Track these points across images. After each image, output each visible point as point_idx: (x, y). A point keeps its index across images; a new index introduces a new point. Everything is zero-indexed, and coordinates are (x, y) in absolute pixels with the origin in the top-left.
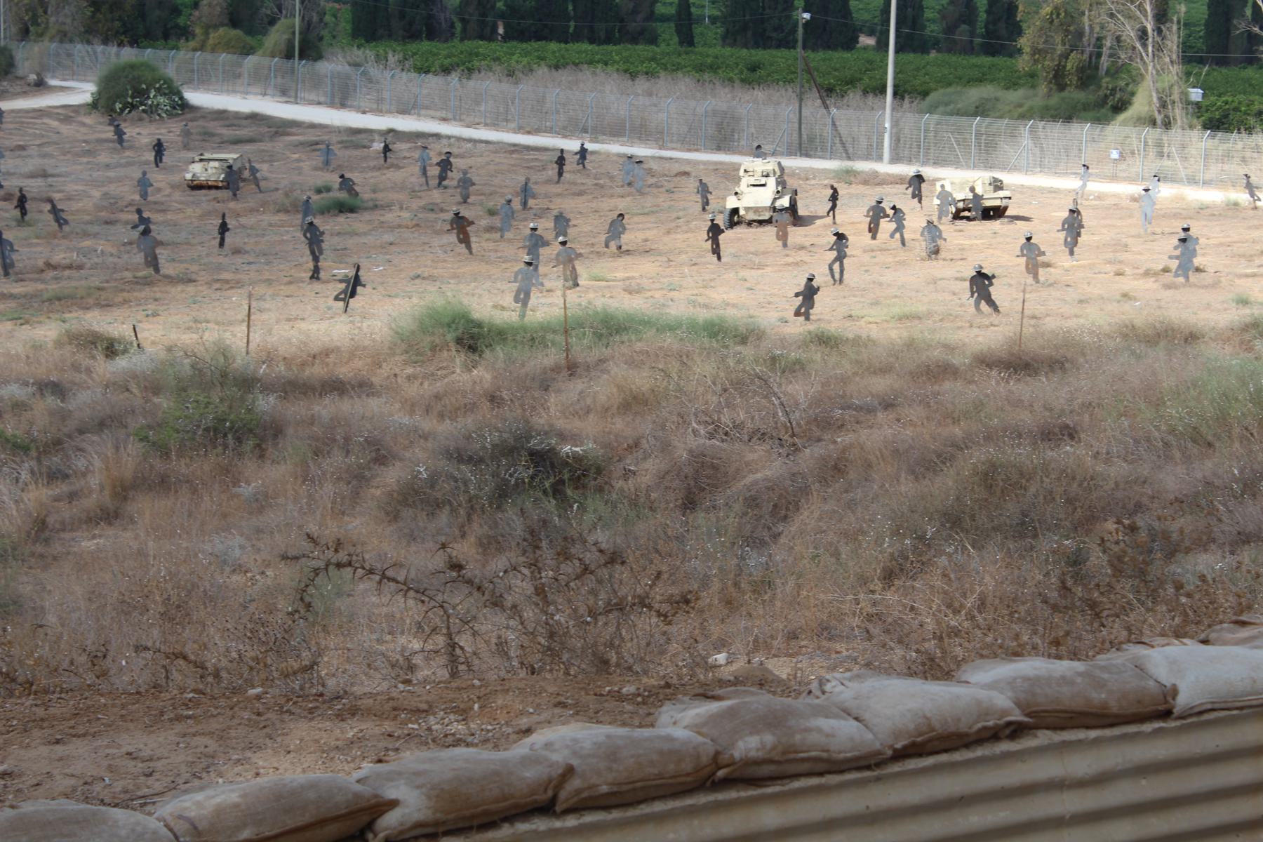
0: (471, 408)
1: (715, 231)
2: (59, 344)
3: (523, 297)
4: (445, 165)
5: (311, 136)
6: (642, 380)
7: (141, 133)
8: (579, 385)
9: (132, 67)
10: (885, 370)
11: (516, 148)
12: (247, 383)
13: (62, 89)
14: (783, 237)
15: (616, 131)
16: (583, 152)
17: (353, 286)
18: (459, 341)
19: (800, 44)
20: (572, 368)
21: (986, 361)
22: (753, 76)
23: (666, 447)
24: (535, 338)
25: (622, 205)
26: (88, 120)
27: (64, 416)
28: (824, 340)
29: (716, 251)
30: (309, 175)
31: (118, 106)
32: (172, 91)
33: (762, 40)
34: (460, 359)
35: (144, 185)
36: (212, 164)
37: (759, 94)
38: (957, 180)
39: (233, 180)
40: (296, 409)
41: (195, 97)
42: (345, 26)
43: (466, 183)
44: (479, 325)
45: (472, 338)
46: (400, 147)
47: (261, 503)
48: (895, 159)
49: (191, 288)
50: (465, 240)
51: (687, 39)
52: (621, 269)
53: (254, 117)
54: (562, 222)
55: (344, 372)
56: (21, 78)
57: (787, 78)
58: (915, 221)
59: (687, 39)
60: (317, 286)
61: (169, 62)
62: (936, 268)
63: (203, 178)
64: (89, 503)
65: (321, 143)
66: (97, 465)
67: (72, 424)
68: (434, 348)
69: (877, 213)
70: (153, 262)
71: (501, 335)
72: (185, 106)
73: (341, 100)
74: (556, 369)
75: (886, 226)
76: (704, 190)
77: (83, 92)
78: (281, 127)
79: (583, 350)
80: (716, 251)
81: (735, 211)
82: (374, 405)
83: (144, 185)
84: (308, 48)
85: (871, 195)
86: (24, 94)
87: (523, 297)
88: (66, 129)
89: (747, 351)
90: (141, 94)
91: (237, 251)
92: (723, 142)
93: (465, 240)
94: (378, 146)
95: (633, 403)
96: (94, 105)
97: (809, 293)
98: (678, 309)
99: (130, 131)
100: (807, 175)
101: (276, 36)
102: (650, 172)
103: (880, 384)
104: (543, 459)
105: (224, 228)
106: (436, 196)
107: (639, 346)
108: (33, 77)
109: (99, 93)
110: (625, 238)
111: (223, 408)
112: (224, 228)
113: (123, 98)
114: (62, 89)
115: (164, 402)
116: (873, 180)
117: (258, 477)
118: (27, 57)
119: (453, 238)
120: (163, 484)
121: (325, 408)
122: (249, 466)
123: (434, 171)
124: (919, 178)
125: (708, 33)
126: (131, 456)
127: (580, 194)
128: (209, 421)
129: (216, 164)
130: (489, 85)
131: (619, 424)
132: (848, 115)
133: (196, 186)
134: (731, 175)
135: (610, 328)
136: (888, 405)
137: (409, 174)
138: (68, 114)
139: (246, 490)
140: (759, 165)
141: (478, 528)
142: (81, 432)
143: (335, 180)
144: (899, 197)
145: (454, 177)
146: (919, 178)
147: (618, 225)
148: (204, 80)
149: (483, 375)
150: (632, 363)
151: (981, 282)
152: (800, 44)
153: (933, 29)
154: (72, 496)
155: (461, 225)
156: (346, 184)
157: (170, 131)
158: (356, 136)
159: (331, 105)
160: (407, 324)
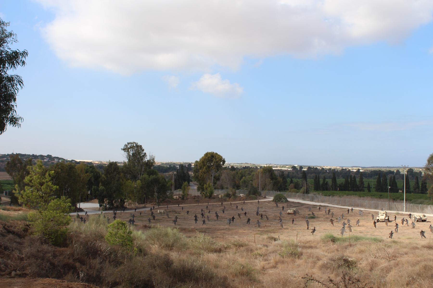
0: (333, 252)
1: (375, 223)
2: (267, 239)
3: (342, 233)
4: (329, 211)
5: (307, 206)
6: (363, 248)
7: (280, 205)
8: (351, 248)
9: (279, 195)
10: (405, 248)
11: (341, 208)
12: (297, 246)
14: (387, 224)
15: (358, 206)
16: (352, 209)
17: (314, 230)
18: (331, 240)
20: (351, 245)
21: (424, 247)
22: (381, 197)
23: (367, 259)
24: (344, 240)
25: (359, 218)
27: (267, 250)
28: (394, 242)
29: (375, 226)
30: (307, 212)
32: (285, 199)
33: (382, 191)
34: (332, 243)
35: (281, 213)
37: (382, 200)
38: (417, 215)
39: (295, 213)
40: (305, 251)
41: (289, 200)
42: (313, 188)
43: (333, 214)
44: (335, 238)
45: (334, 240)
46: (322, 208)
47: (299, 266)
48: (406, 211)
49: (288, 230)
50: (332, 223)
51: (369, 191)
52: (359, 229)
53: (298, 203)
54: (349, 221)
55: (312, 245)
57: (387, 197)
58: (410, 222)
59: (369, 191)
60: (308, 230)
61: (285, 194)
62: (414, 230)
64: (271, 265)
65: (309, 207)
66: (272, 259)
67: (269, 252)
68: (327, 241)
69: (403, 220)
70: (282, 226)
71: (338, 239)
72: (287, 201)
73: (312, 200)
74: (348, 245)
75: (405, 223)
76: (373, 216)
77: (272, 199)
78: (302, 205)
79: (353, 242)
80: (375, 226)
81: (378, 219)
82: (317, 250)
83: (281, 213)
84: (307, 192)
85: (402, 217)
86: (262, 199)
87: (342, 233)
88: (269, 204)
89: (381, 244)
91: (295, 224)
92: (376, 208)
93: (332, 223)
94: (318, 208)
95: (361, 252)
96: (273, 201)
97: (392, 234)
98: (368, 236)
99: (279, 205)
100: (391, 214)
101: (302, 190)
102: (363, 213)
103: (405, 250)
104: (346, 261)
105: (293, 221)
106: (328, 216)
107: (362, 242)
110: (359, 224)
111: (293, 250)
112: (293, 221)
113: (278, 200)
115: (283, 249)
116: (402, 215)
117: (299, 262)
118: (263, 193)
119: (330, 223)
120: (283, 262)
121: (309, 251)
122: (297, 260)
123: (327, 212)
124: (410, 215)
125: (373, 190)
126: (278, 257)
127: (352, 216)
128: (290, 252)
130: (336, 198)
131: (359, 255)
132: (396, 204)
133: (289, 214)
134: (377, 213)
135: (357, 239)
136: (406, 254)
137: (323, 212)
138: (269, 202)
139: (296, 264)
140: (382, 212)
141: (335, 272)
142: (270, 253)
143: (311, 213)
144: (407, 218)
145: (331, 213)
146: (410, 215)
147: (358, 221)
148: (290, 197)
149: (335, 246)
150: (361, 245)
151: (422, 233)
153: (412, 189)
154: (269, 263)
155: (332, 221)
156: (313, 214)
157: (285, 205)
158: (315, 206)
159: (311, 201)
160: (323, 237)
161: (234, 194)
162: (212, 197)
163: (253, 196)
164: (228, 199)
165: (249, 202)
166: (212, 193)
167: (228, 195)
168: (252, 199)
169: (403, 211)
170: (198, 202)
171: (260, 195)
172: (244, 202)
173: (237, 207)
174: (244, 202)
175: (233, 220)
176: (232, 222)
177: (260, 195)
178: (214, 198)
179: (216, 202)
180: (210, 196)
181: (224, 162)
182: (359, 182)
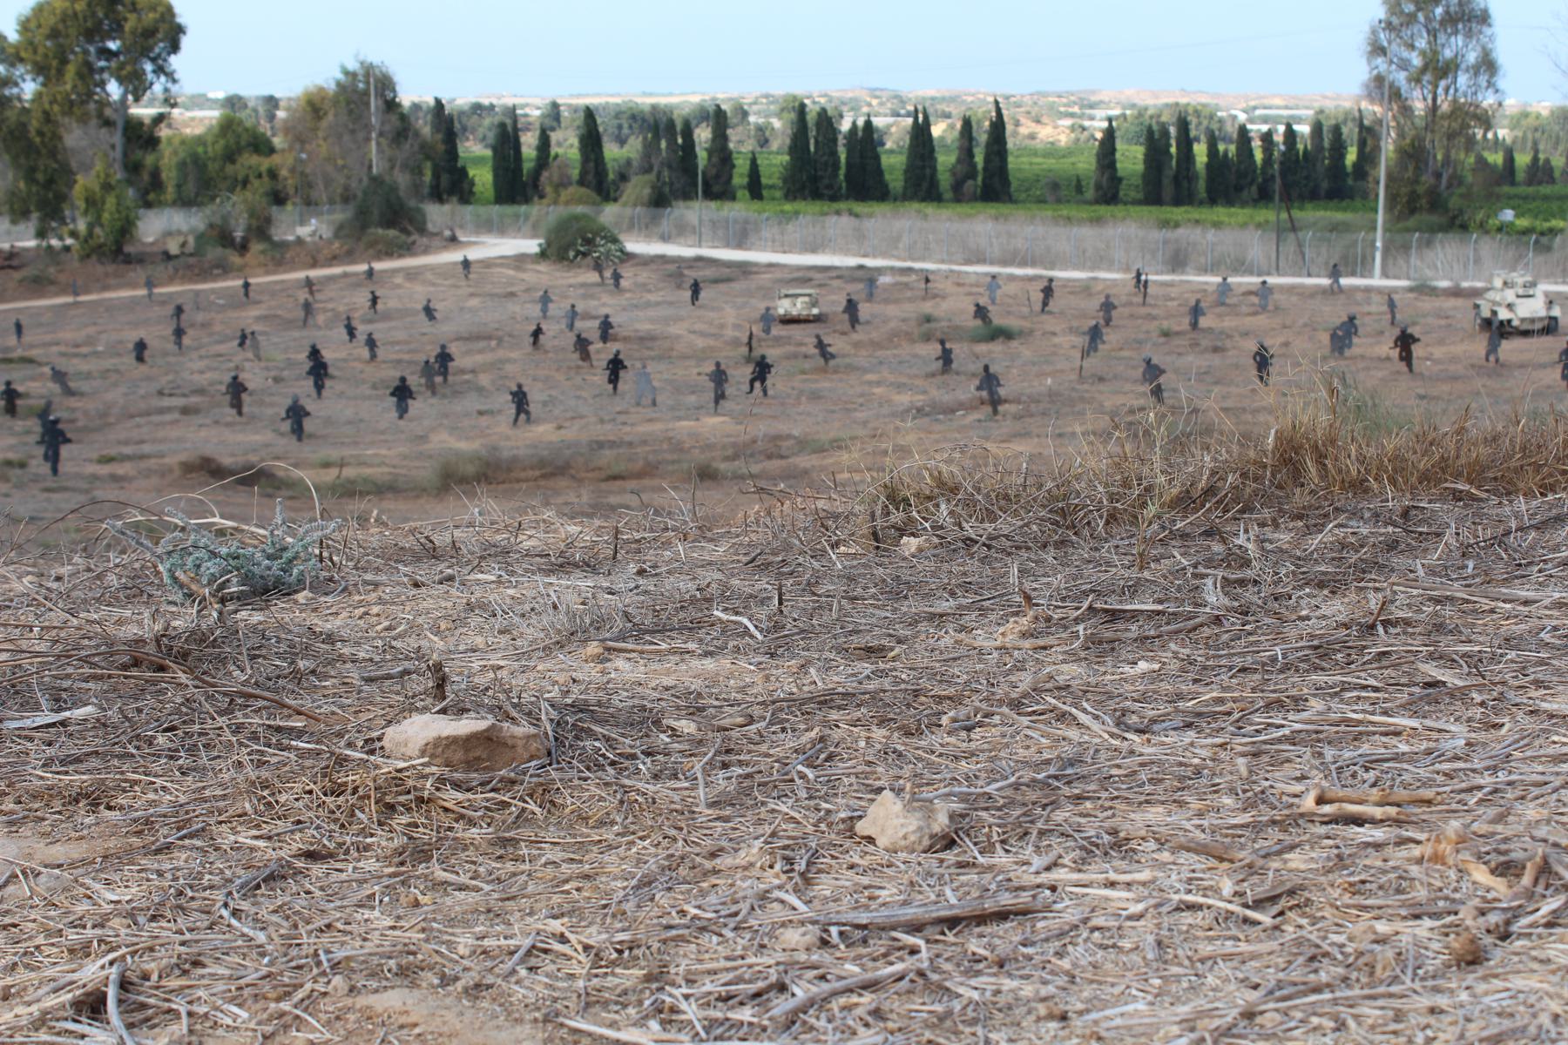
13: (475, 243)
19: (1277, 197)
26: (543, 267)
31: (571, 254)
32: (615, 241)
36: (800, 299)
53: (699, 259)
56: (436, 234)
63: (794, 313)
86: (445, 248)
90: (589, 242)
96: (543, 255)
108: (447, 233)
109: (549, 244)
114: (475, 243)
129: (807, 299)
152: (1277, 197)
161: (261, 229)
162: (128, 249)
163: (392, 233)
164: (236, 259)
165: (395, 271)
166: (125, 230)
167: (223, 237)
168: (389, 254)
169: (1371, 276)
170: (39, 285)
171: (422, 230)
172: (370, 273)
173: (374, 300)
174: (370, 273)
175: (444, 373)
176: (439, 379)
177: (422, 230)
178: (140, 260)
179: (171, 280)
180: (116, 250)
181: (175, 47)
182: (710, 152)
